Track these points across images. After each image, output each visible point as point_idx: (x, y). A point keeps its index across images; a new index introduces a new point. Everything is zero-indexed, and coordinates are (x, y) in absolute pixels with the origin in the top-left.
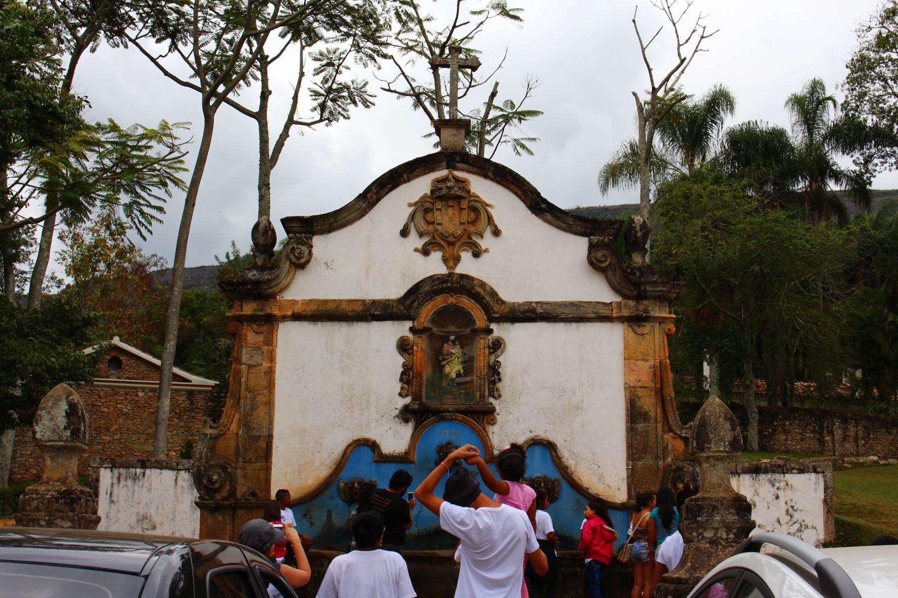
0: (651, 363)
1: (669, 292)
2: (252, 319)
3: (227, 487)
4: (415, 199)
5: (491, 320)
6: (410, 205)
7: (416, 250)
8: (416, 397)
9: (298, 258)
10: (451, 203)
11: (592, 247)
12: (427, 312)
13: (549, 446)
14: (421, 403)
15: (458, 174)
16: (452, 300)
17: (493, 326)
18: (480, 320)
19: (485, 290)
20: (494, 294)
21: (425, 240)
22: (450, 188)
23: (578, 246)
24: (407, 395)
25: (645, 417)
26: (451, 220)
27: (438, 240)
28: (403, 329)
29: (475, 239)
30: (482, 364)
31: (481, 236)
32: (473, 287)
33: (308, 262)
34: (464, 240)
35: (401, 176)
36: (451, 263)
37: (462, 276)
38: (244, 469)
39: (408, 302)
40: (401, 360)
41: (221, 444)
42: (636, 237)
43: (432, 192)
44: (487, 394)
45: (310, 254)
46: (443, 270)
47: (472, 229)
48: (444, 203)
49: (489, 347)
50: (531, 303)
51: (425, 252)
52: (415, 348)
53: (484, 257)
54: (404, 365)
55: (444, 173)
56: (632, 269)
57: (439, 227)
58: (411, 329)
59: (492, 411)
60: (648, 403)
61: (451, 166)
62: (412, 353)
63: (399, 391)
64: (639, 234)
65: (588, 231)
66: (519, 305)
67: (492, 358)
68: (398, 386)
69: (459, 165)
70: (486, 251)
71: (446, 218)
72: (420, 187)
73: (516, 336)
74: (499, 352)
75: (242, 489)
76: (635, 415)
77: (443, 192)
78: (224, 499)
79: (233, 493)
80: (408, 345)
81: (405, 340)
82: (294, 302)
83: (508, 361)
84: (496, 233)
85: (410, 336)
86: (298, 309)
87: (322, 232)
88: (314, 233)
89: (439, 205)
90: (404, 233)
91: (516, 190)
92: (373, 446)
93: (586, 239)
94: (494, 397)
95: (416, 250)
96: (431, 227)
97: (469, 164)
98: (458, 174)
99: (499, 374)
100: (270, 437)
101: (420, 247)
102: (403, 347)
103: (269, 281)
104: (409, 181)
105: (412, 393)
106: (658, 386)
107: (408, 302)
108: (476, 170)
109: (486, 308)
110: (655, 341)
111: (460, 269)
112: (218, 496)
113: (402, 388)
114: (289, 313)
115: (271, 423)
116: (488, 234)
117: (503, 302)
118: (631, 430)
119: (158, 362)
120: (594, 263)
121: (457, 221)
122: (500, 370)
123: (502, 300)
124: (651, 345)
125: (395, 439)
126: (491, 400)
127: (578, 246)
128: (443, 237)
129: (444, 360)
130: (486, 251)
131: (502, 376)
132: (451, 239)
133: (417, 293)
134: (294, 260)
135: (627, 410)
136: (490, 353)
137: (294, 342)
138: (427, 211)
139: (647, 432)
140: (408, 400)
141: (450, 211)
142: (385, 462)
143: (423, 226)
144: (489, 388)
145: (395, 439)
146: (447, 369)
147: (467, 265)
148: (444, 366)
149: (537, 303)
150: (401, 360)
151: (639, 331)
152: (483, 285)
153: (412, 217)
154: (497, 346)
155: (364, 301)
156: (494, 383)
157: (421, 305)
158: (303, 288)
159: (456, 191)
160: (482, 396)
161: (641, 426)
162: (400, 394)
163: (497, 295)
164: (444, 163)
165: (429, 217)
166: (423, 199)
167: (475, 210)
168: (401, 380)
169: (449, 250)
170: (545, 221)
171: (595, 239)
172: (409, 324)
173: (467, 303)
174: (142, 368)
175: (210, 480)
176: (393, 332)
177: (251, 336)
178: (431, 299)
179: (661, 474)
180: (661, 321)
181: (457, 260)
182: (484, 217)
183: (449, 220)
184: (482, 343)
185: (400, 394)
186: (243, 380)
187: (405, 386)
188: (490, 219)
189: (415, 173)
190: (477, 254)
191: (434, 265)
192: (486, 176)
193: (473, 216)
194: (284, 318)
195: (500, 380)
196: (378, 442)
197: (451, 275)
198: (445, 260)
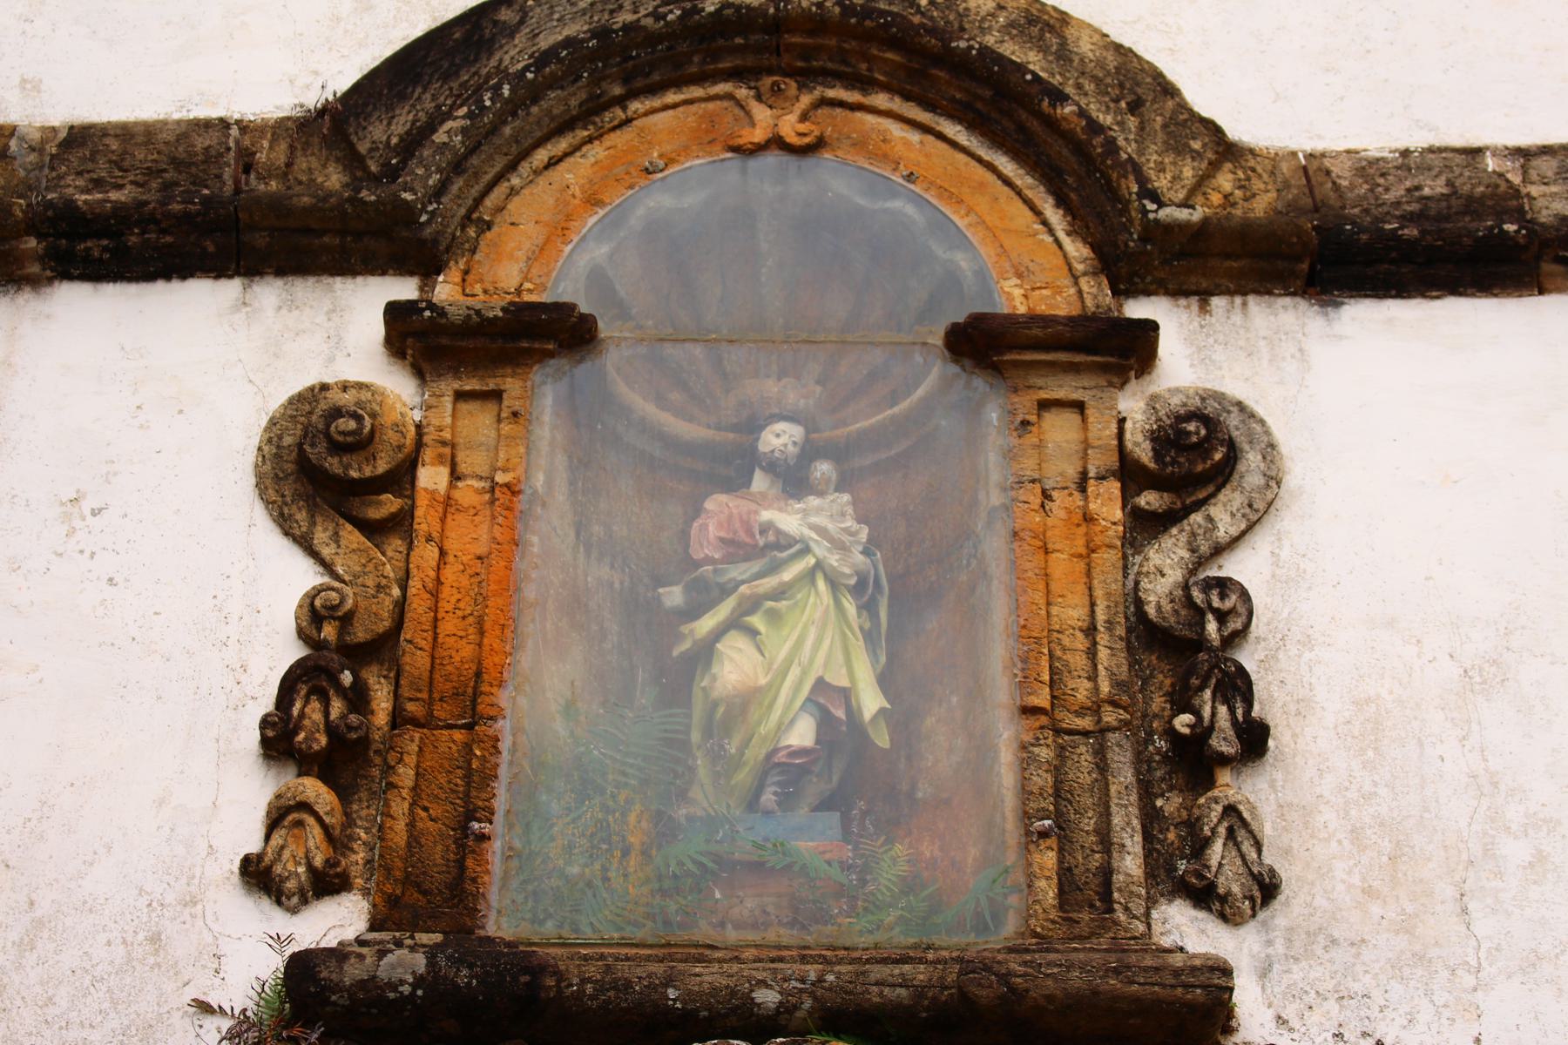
19: (1063, 55)
24: (326, 884)
30: (1072, 613)
39: (382, 132)
40: (292, 577)
44: (1131, 864)
49: (1129, 474)
50: (1475, 153)
52: (431, 477)
54: (314, 614)
62: (401, 523)
63: (252, 842)
66: (1369, 169)
67: (1165, 566)
68: (238, 800)
74: (1223, 514)
80: (361, 444)
81: (337, 412)
83: (1320, 593)
85: (399, 390)
94: (1204, 896)
99: (1237, 686)
102: (323, 470)
105: (380, 865)
107: (382, 132)
113: (280, 816)
117: (1226, 150)
122: (1248, 657)
123: (1213, 129)
126: (1185, 929)
129: (703, 597)
131: (1270, 702)
136: (1145, 527)
140: (338, 921)
144: (1151, 820)
146: (737, 664)
148: (705, 653)
149: (1523, 154)
150: (292, 577)
154: (1198, 461)
156: (1194, 763)
162: (258, 875)
163: (1168, 90)
168: (278, 741)
176: (244, 354)
185: (258, 875)
187: (314, 789)
195: (1254, 740)
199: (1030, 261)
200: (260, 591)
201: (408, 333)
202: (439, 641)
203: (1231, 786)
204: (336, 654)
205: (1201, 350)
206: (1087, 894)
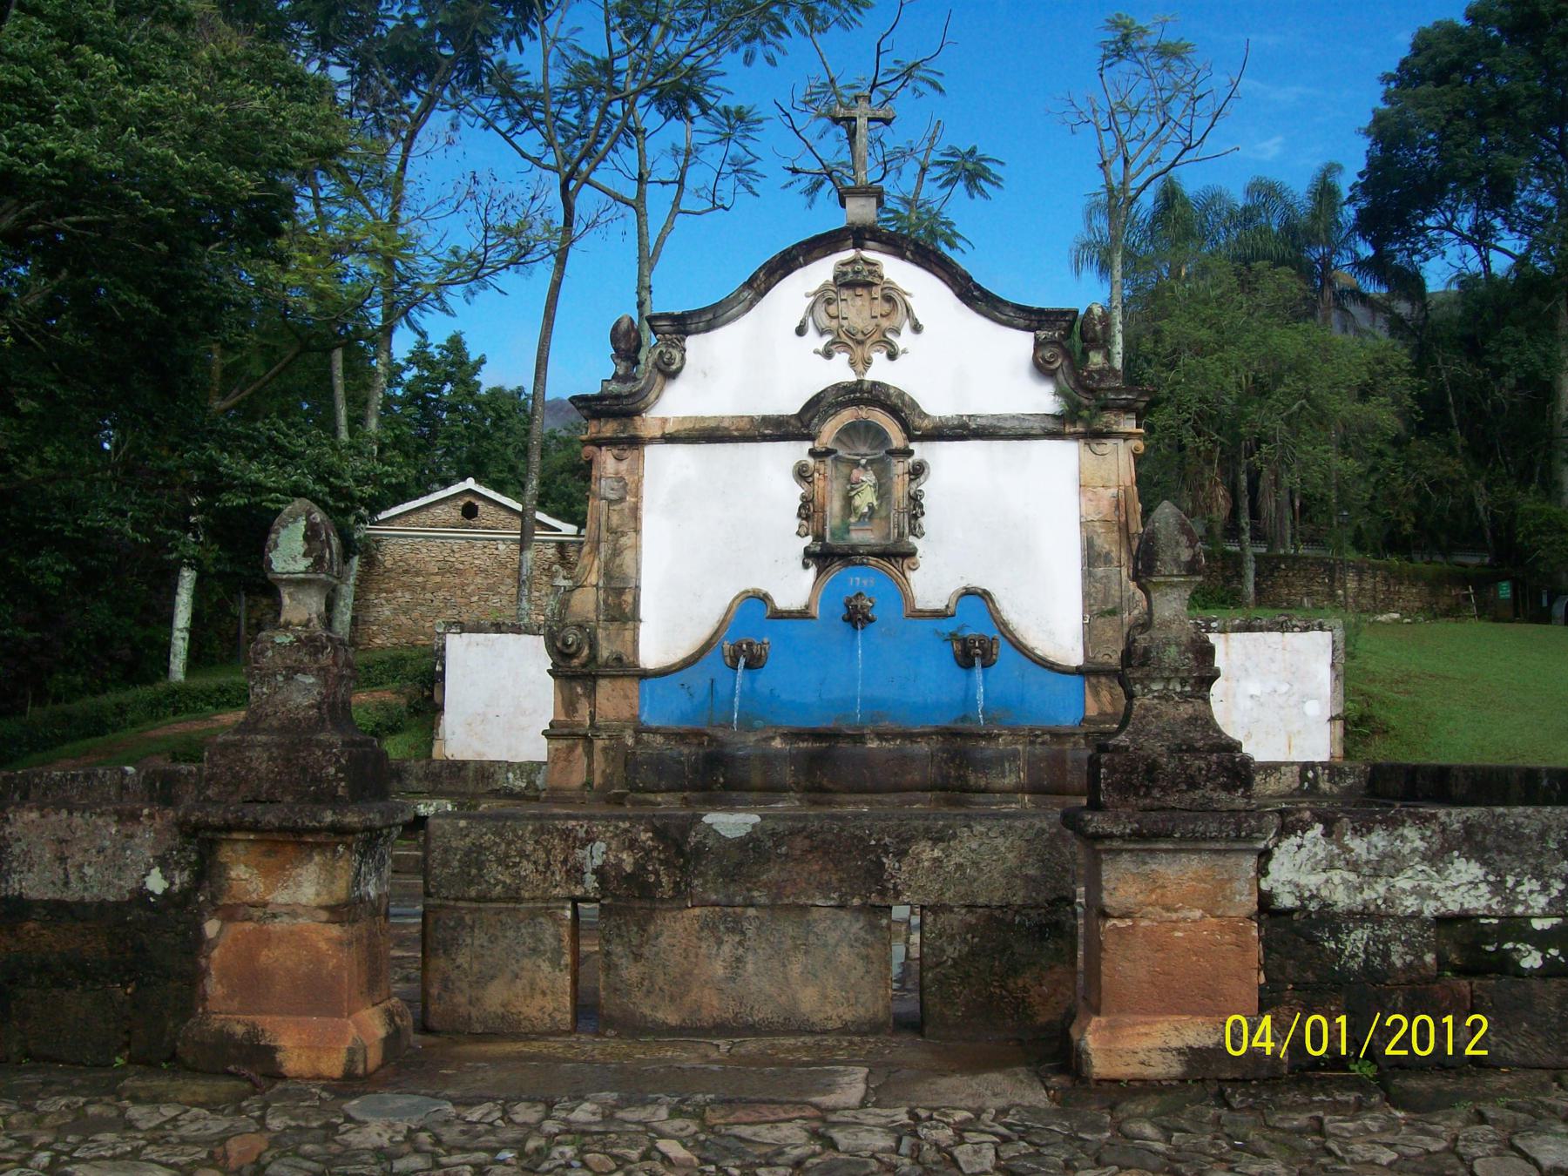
0: (1113, 491)
1: (1136, 401)
2: (611, 442)
3: (586, 651)
4: (815, 288)
5: (912, 438)
6: (807, 296)
7: (816, 352)
8: (819, 537)
9: (669, 364)
10: (859, 291)
11: (1038, 345)
12: (829, 431)
13: (985, 595)
14: (824, 545)
15: (866, 254)
16: (865, 413)
17: (913, 446)
18: (897, 438)
20: (914, 405)
21: (828, 338)
22: (856, 273)
23: (1021, 343)
25: (1107, 559)
26: (859, 313)
27: (845, 338)
28: (797, 451)
29: (889, 336)
31: (897, 332)
32: (888, 396)
33: (679, 370)
34: (876, 337)
35: (796, 258)
36: (860, 367)
37: (874, 384)
38: (606, 629)
41: (577, 597)
42: (1095, 331)
43: (835, 278)
45: (683, 359)
46: (850, 377)
47: (885, 323)
48: (851, 292)
51: (828, 354)
53: (901, 359)
54: (803, 497)
55: (849, 254)
56: (1090, 373)
57: (845, 323)
58: (812, 453)
59: (911, 554)
60: (1107, 542)
61: (858, 245)
64: (1098, 328)
65: (1035, 324)
67: (914, 485)
68: (795, 523)
69: (870, 244)
70: (904, 352)
71: (854, 311)
72: (822, 271)
73: (942, 458)
75: (605, 653)
76: (1092, 557)
77: (850, 277)
78: (584, 665)
79: (593, 657)
82: (664, 421)
84: (917, 328)
85: (811, 461)
86: (670, 428)
87: (697, 332)
88: (688, 333)
89: (845, 294)
90: (801, 331)
91: (942, 274)
92: (764, 598)
93: (1032, 335)
95: (816, 352)
96: (834, 323)
97: (880, 242)
98: (866, 254)
99: (921, 506)
100: (638, 588)
101: (821, 349)
102: (802, 474)
103: (631, 395)
104: (806, 263)
106: (1123, 519)
108: (890, 249)
109: (905, 426)
110: (1117, 462)
111: (871, 375)
112: (576, 662)
114: (658, 434)
115: (638, 571)
116: (906, 329)
117: (926, 416)
118: (1088, 575)
119: (518, 507)
120: (1042, 368)
121: (866, 314)
124: (1114, 467)
125: (794, 587)
126: (912, 539)
127: (1021, 343)
128: (849, 334)
130: (904, 352)
132: (860, 337)
133: (820, 406)
134: (663, 366)
135: (1083, 550)
136: (911, 480)
137: (665, 469)
138: (829, 302)
139: (1107, 577)
141: (859, 302)
142: (782, 618)
143: (825, 322)
145: (794, 587)
146: (857, 501)
147: (881, 371)
151: (1099, 449)
152: (901, 394)
153: (811, 309)
154: (918, 471)
155: (751, 418)
156: (916, 517)
157: (823, 421)
158: (676, 403)
159: (865, 276)
160: (901, 535)
161: (1100, 571)
162: (798, 533)
164: (850, 242)
165: (832, 309)
166: (824, 288)
167: (888, 299)
168: (799, 515)
169: (859, 350)
170: (979, 312)
171: (1042, 334)
172: (808, 445)
173: (880, 417)
174: (503, 514)
175: (565, 644)
177: (607, 462)
178: (836, 413)
179: (1126, 629)
180: (1127, 436)
181: (867, 363)
182: (901, 308)
183: (857, 311)
184: (900, 467)
185: (798, 533)
186: (603, 519)
188: (908, 310)
189: (815, 254)
190: (892, 356)
191: (839, 371)
192: (903, 257)
193: (887, 307)
194: (652, 440)
196: (771, 594)
197: (860, 382)
198: (852, 364)
199: (897, 438)
200: (796, 492)
201: (812, 453)
202: (818, 500)
203: (922, 520)
204: (806, 502)
205: (920, 450)
206: (901, 535)
